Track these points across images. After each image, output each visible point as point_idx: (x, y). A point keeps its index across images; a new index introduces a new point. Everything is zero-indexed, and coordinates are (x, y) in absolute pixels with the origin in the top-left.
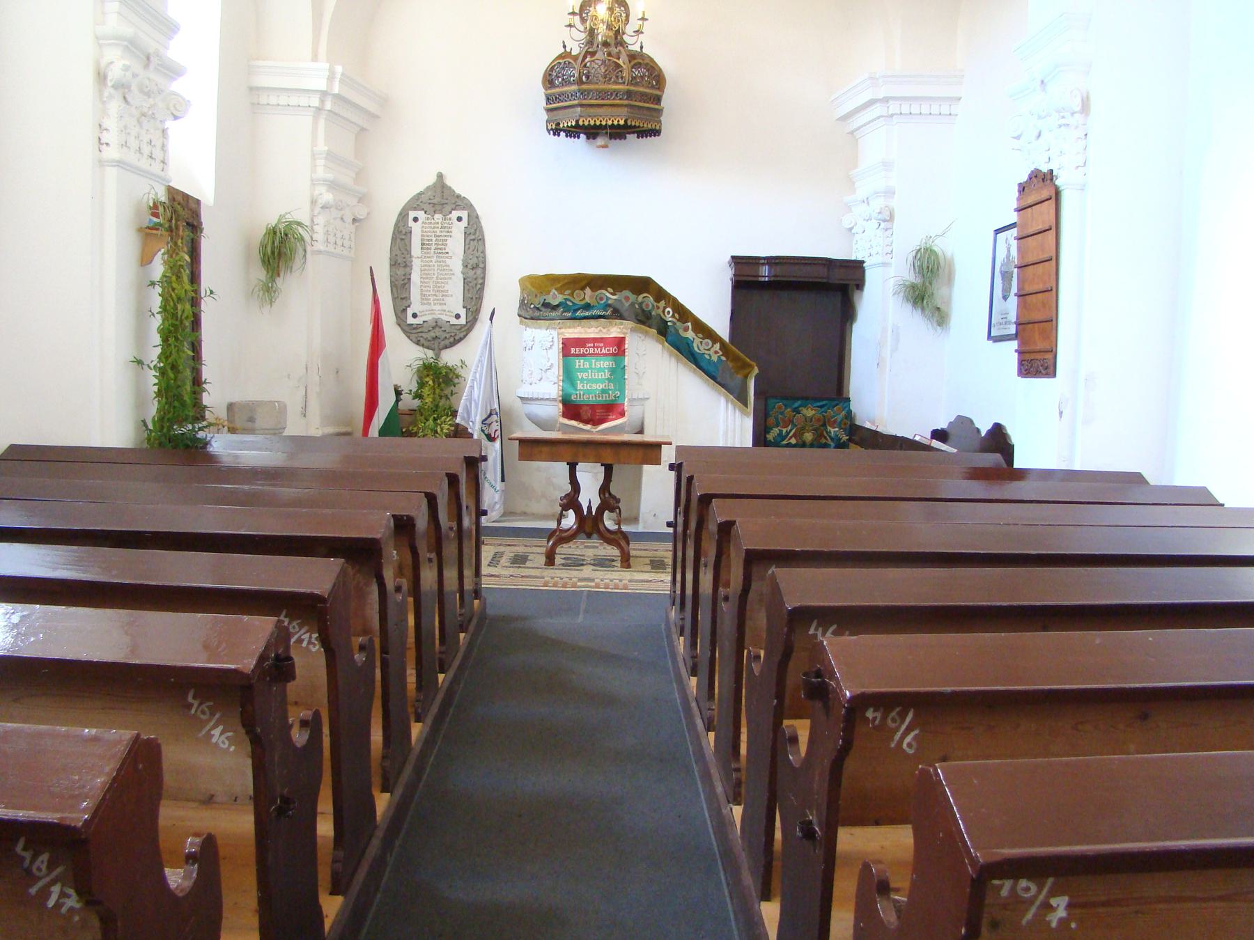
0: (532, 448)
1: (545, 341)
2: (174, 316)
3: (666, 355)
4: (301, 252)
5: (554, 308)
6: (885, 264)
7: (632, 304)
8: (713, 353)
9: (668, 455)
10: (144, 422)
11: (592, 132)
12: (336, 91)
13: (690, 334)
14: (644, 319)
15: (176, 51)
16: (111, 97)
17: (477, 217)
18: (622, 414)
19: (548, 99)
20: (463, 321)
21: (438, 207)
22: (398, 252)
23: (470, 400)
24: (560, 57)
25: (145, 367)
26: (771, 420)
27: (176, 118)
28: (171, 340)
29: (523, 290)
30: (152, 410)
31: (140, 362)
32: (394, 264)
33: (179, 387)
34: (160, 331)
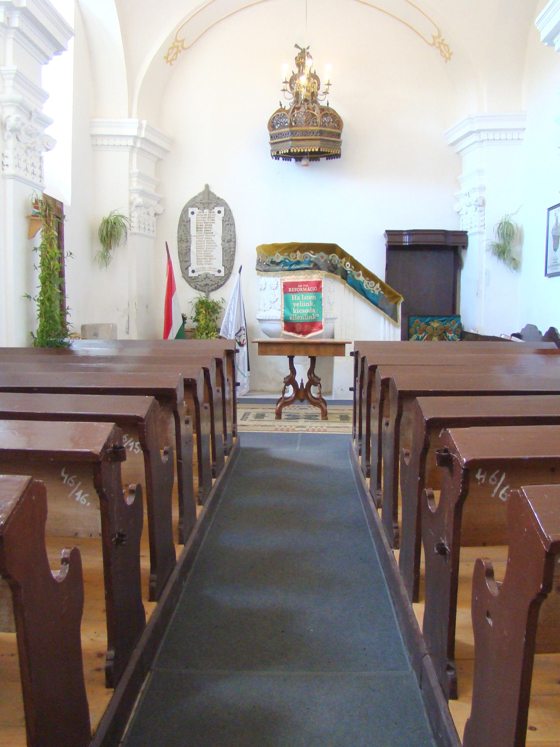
0: (266, 347)
1: (274, 282)
2: (49, 268)
3: (347, 292)
4: (124, 234)
5: (278, 264)
6: (480, 233)
7: (326, 261)
8: (376, 289)
9: (349, 349)
10: (32, 333)
11: (298, 157)
12: (143, 135)
13: (361, 278)
14: (333, 269)
15: (47, 110)
16: (9, 137)
17: (230, 211)
18: (321, 328)
19: (271, 137)
20: (222, 274)
21: (206, 205)
22: (182, 233)
23: (228, 321)
24: (279, 111)
25: (32, 300)
26: (412, 330)
27: (48, 150)
28: (47, 283)
29: (259, 253)
30: (37, 326)
31: (29, 297)
32: (180, 240)
33: (52, 311)
34: (41, 278)
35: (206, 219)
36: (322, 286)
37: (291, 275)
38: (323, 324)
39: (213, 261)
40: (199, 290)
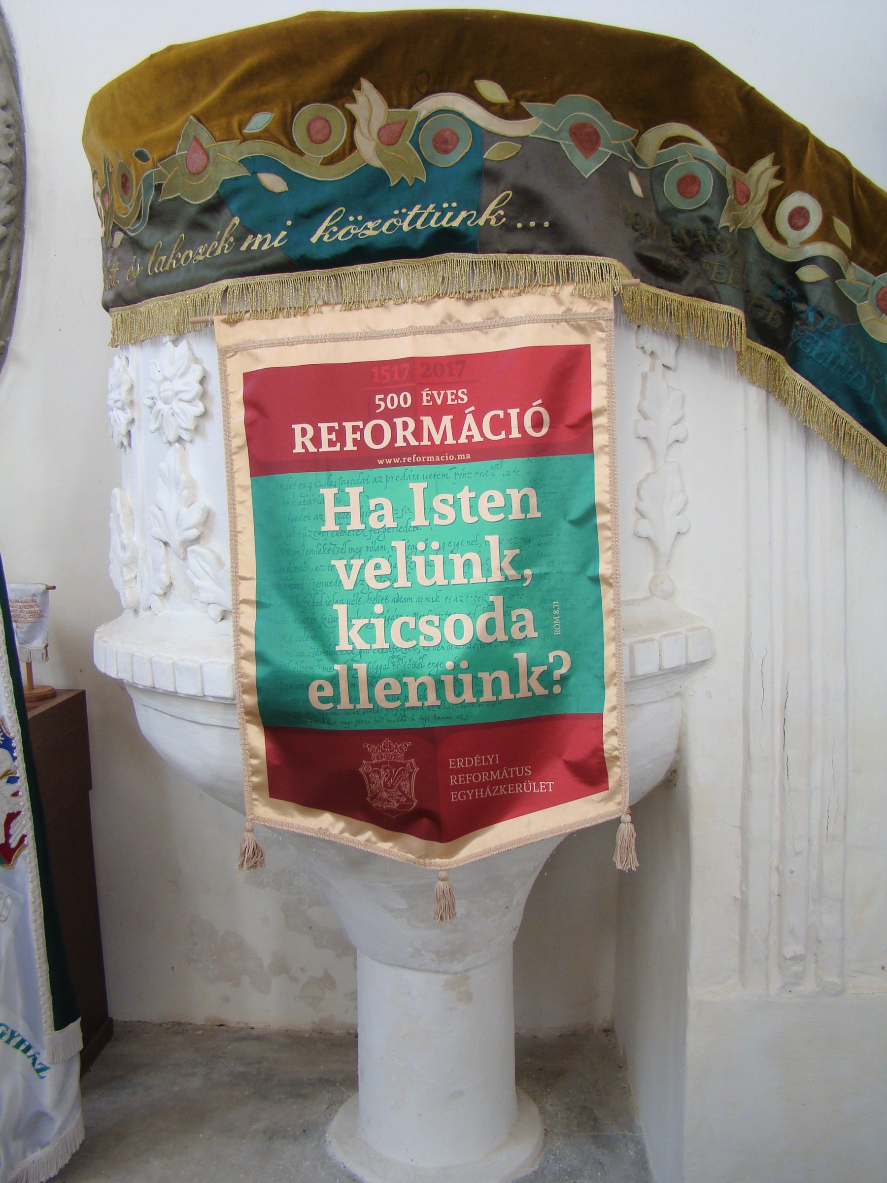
7: (613, 173)
14: (674, 257)
36: (598, 398)
37: (303, 310)
38: (610, 744)
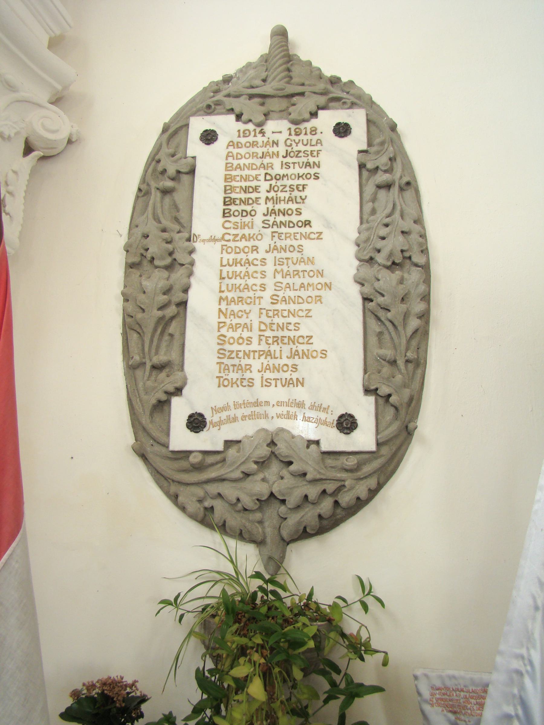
17: (393, 127)
20: (364, 439)
22: (152, 227)
35: (277, 162)
39: (308, 368)
40: (223, 528)
